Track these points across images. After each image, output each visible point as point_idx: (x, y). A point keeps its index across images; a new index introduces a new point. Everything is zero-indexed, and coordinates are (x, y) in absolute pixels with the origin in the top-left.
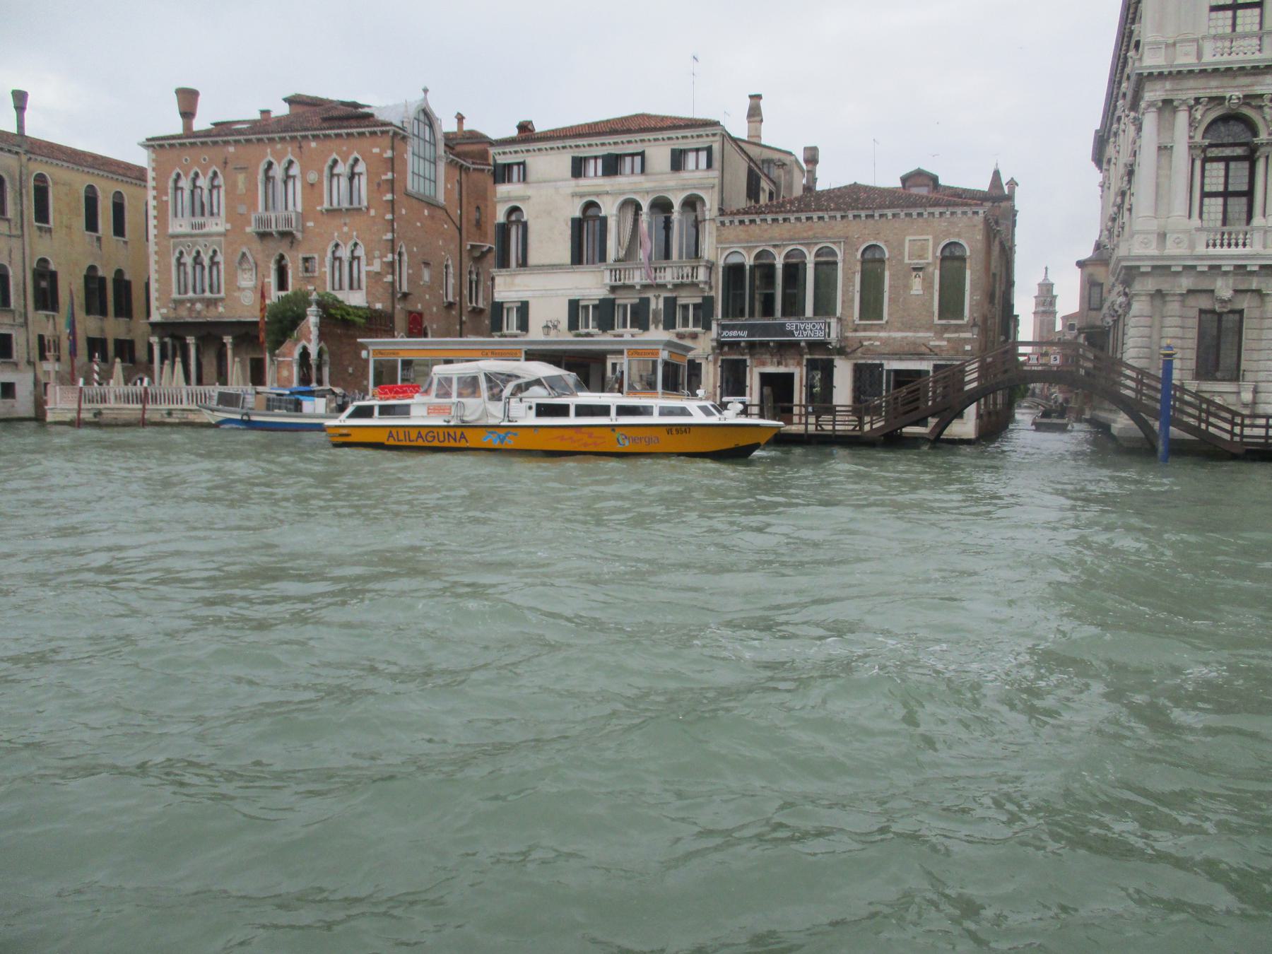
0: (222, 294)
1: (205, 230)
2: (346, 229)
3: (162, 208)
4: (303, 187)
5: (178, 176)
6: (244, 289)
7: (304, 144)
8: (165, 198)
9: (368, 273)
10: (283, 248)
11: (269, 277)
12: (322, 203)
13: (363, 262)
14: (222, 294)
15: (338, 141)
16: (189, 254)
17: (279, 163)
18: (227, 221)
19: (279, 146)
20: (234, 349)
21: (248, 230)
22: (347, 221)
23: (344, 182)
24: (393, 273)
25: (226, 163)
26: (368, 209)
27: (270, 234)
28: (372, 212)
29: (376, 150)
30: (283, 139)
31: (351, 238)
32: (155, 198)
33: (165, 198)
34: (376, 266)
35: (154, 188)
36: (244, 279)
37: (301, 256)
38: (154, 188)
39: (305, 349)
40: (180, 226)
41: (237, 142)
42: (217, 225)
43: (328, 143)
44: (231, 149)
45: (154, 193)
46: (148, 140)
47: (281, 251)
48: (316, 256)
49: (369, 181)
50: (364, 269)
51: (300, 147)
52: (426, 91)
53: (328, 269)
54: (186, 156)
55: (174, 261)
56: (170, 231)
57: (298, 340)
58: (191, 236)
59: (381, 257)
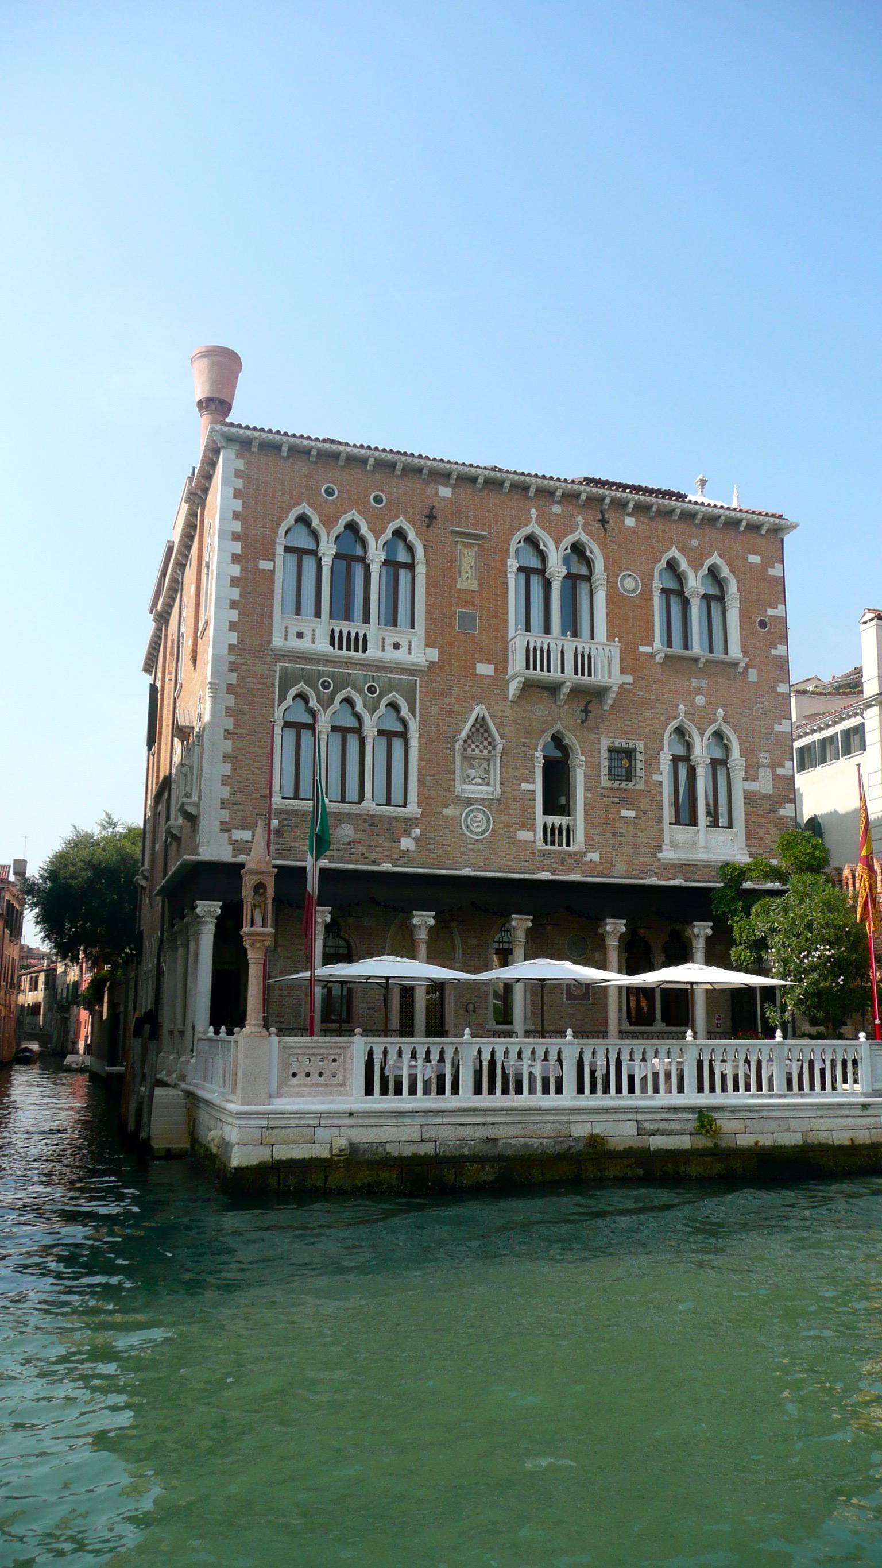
0: (413, 809)
1: (373, 652)
2: (700, 700)
4: (609, 602)
6: (469, 802)
8: (265, 565)
9: (749, 797)
12: (650, 642)
15: (681, 527)
18: (429, 643)
19: (557, 509)
22: (704, 683)
25: (431, 517)
27: (552, 689)
28: (753, 675)
31: (715, 720)
33: (265, 565)
34: (764, 784)
36: (467, 779)
37: (605, 743)
44: (445, 492)
47: (559, 726)
48: (640, 746)
50: (740, 787)
51: (604, 521)
55: (278, 713)
58: (334, 663)
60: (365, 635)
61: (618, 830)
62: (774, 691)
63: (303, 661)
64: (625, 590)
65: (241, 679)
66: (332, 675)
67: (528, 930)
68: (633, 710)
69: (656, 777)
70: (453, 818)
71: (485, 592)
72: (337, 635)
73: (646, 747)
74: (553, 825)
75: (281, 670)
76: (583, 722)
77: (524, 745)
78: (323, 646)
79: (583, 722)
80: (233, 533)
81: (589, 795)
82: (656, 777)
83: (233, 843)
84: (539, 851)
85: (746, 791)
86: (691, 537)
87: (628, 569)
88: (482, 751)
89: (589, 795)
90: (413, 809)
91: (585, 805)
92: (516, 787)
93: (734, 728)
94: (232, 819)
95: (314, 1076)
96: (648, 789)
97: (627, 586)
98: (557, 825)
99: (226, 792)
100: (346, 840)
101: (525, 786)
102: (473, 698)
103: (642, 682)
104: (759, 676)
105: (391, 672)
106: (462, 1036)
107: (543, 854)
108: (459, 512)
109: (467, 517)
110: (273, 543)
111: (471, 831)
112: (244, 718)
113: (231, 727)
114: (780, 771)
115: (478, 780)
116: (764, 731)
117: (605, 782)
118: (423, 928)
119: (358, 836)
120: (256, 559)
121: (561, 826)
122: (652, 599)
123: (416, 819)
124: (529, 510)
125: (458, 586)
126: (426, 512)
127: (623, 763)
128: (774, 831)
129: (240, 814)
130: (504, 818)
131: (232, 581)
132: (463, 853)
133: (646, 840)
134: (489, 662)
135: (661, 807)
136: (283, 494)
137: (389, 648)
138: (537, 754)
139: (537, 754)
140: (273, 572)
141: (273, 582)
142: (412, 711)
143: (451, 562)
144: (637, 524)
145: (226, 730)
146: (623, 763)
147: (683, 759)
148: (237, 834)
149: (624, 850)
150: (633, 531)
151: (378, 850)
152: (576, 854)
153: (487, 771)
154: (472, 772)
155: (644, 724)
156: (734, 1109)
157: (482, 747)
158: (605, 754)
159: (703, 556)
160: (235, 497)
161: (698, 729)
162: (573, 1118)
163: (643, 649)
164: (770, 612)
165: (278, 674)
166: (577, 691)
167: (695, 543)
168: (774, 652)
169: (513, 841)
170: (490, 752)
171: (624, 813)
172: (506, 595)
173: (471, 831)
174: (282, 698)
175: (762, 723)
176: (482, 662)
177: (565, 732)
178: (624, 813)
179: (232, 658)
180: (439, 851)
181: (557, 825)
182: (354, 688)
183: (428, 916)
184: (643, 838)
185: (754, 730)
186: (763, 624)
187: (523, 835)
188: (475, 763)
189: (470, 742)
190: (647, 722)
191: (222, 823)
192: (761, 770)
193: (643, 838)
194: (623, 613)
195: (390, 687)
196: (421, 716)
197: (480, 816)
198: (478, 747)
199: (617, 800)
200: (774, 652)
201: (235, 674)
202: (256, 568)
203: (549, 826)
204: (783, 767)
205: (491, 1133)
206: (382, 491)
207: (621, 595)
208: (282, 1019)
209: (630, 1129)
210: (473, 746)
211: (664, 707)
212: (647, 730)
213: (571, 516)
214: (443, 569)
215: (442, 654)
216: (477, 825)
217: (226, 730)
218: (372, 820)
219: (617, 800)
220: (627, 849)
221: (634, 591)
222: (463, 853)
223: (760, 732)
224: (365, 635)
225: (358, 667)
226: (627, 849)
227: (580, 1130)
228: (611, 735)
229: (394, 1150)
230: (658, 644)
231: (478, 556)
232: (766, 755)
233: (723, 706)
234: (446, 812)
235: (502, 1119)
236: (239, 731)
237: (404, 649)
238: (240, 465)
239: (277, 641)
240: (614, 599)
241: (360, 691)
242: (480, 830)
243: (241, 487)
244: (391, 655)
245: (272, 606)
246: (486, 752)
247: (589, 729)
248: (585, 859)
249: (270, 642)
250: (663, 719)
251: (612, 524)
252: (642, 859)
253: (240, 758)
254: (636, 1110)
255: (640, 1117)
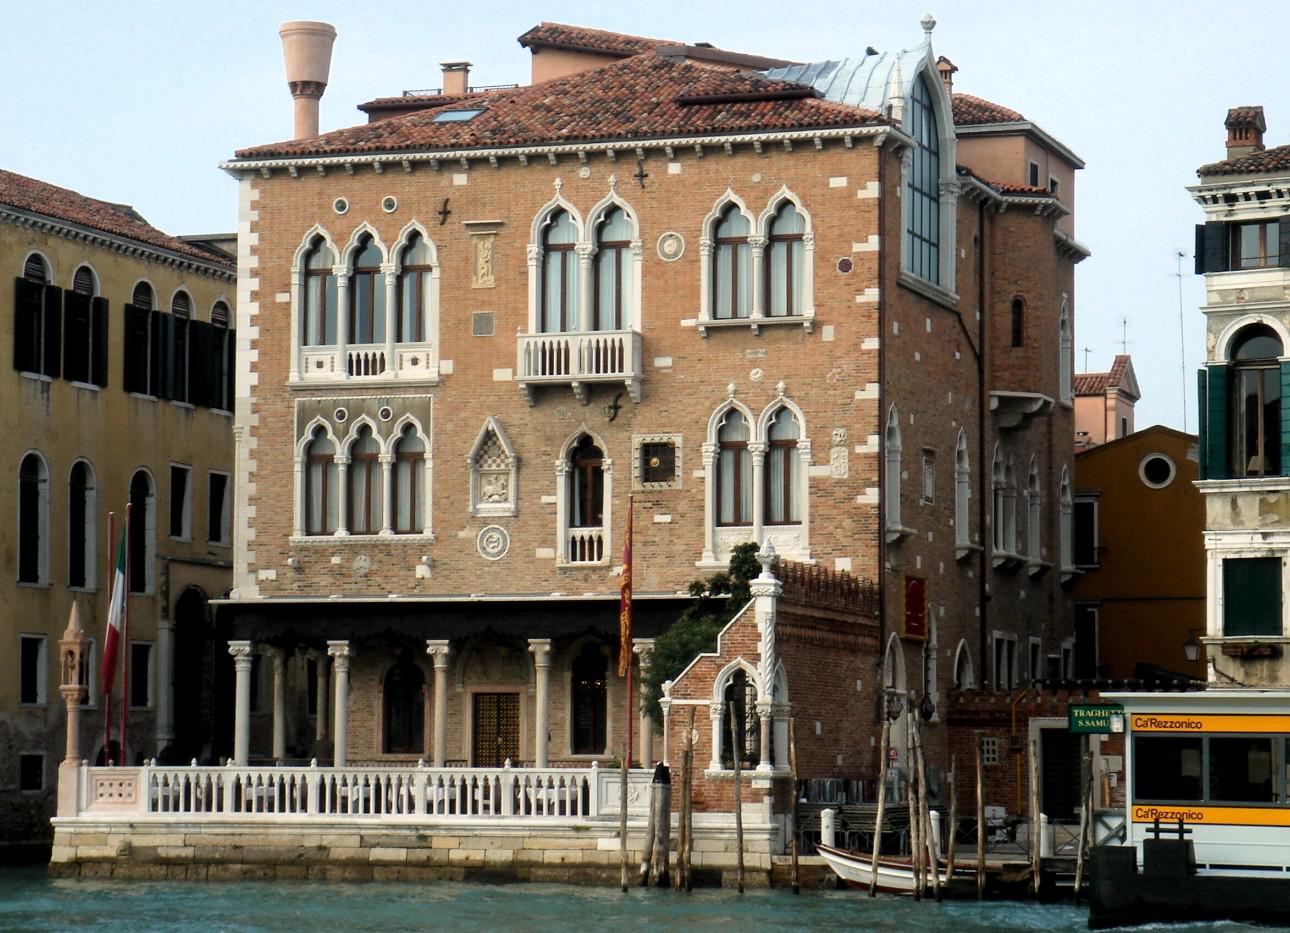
2: (756, 374)
3: (271, 321)
4: (645, 273)
5: (318, 241)
6: (485, 521)
7: (651, 167)
8: (281, 298)
9: (817, 487)
10: (591, 420)
11: (551, 491)
12: (694, 312)
13: (802, 455)
14: (428, 534)
15: (741, 160)
16: (341, 434)
17: (585, 212)
18: (443, 356)
19: (584, 172)
20: (449, 673)
21: (501, 375)
23: (751, 260)
24: (881, 485)
25: (445, 213)
26: (816, 325)
27: (566, 387)
28: (828, 333)
29: (838, 182)
30: (592, 157)
31: (774, 397)
32: (255, 296)
33: (281, 298)
34: (837, 467)
35: (254, 273)
37: (637, 440)
38: (254, 273)
39: (740, 675)
40: (324, 366)
41: (473, 163)
42: (416, 364)
43: (712, 164)
44: (460, 179)
45: (254, 284)
46: (243, 156)
47: (584, 428)
49: (820, 258)
50: (804, 472)
51: (642, 176)
52: (929, 25)
53: (708, 474)
54: (341, 190)
56: (294, 378)
57: (729, 654)
59: (849, 443)
60: (382, 355)
61: (649, 539)
62: (857, 345)
63: (320, 393)
64: (666, 255)
65: (263, 420)
66: (347, 404)
67: (547, 653)
68: (671, 399)
69: (697, 474)
70: (469, 541)
71: (503, 288)
72: (354, 359)
73: (686, 440)
74: (582, 538)
75: (299, 405)
76: (612, 420)
77: (545, 453)
78: (338, 375)
79: (612, 420)
80: (251, 270)
81: (617, 502)
82: (697, 474)
83: (260, 583)
84: (561, 568)
85: (812, 480)
86: (753, 171)
87: (669, 229)
88: (498, 466)
89: (617, 502)
90: (428, 534)
91: (613, 514)
92: (536, 501)
93: (800, 402)
94: (257, 559)
95: (116, 796)
96: (686, 488)
97: (667, 250)
98: (586, 538)
99: (251, 534)
100: (363, 572)
101: (545, 499)
102: (489, 408)
103: (684, 363)
104: (837, 332)
105: (405, 392)
106: (503, 766)
107: (564, 570)
108: (475, 200)
109: (484, 205)
110: (289, 274)
111: (488, 554)
112: (266, 458)
113: (254, 469)
114: (860, 449)
115: (495, 497)
116: (840, 402)
117: (637, 486)
118: (439, 657)
119: (374, 567)
120: (273, 294)
121: (591, 538)
122: (698, 261)
123: (431, 544)
124: (553, 181)
125: (474, 286)
126: (440, 208)
127: (658, 461)
128: (848, 523)
129: (265, 554)
130: (523, 536)
131: (252, 320)
132: (479, 577)
133: (683, 548)
134: (507, 365)
135: (702, 508)
136: (297, 219)
137: (407, 364)
138: (558, 463)
139: (558, 463)
140: (288, 304)
141: (288, 316)
142: (426, 431)
143: (467, 259)
144: (683, 170)
145: (250, 473)
146: (658, 461)
147: (730, 449)
148: (264, 575)
149: (658, 560)
150: (678, 179)
151: (395, 579)
152: (601, 568)
153: (504, 487)
154: (489, 489)
155: (684, 414)
156: (449, 828)
157: (498, 461)
158: (637, 454)
159: (767, 193)
160: (252, 231)
161: (752, 410)
162: (305, 831)
163: (685, 323)
164: (857, 248)
165: (296, 410)
166: (592, 390)
167: (756, 178)
168: (860, 299)
169: (531, 559)
170: (507, 465)
171: (658, 518)
172: (525, 286)
173: (488, 554)
174: (301, 433)
175: (838, 392)
176: (499, 367)
177: (593, 435)
178: (658, 518)
179: (254, 400)
180: (454, 576)
181: (586, 538)
182: (368, 414)
183: (443, 645)
184: (679, 547)
185: (827, 402)
186: (845, 266)
187: (543, 553)
188: (492, 478)
189: (486, 457)
190: (690, 409)
191: (249, 564)
192: (833, 450)
193: (679, 546)
194: (661, 282)
195: (404, 409)
196: (436, 434)
197: (496, 536)
198: (494, 461)
199: (649, 505)
200: (860, 299)
201: (257, 416)
202: (274, 303)
203: (578, 539)
204: (865, 443)
205: (237, 841)
206: (393, 194)
207: (659, 263)
208: (356, 750)
209: (355, 841)
210: (490, 461)
211: (710, 389)
212: (688, 419)
213: (603, 178)
214: (458, 269)
215: (456, 364)
216: (493, 546)
217: (250, 473)
218: (386, 548)
219: (649, 505)
220: (661, 560)
221: (676, 254)
222: (479, 577)
223: (835, 404)
224: (382, 355)
225: (373, 391)
226: (661, 560)
227: (311, 842)
228: (642, 430)
229: (162, 853)
230: (704, 317)
231: (493, 248)
232: (841, 431)
233: (786, 377)
234: (462, 534)
235: (247, 831)
236: (262, 473)
237: (422, 363)
238: (255, 195)
239: (294, 378)
240: (653, 269)
241: (374, 417)
242: (496, 550)
243: (256, 218)
244: (410, 374)
245: (289, 339)
246: (503, 466)
247: (620, 427)
248: (611, 574)
249: (287, 378)
250: (707, 403)
251: (652, 176)
252: (678, 570)
253: (264, 499)
254: (358, 826)
255: (363, 832)
